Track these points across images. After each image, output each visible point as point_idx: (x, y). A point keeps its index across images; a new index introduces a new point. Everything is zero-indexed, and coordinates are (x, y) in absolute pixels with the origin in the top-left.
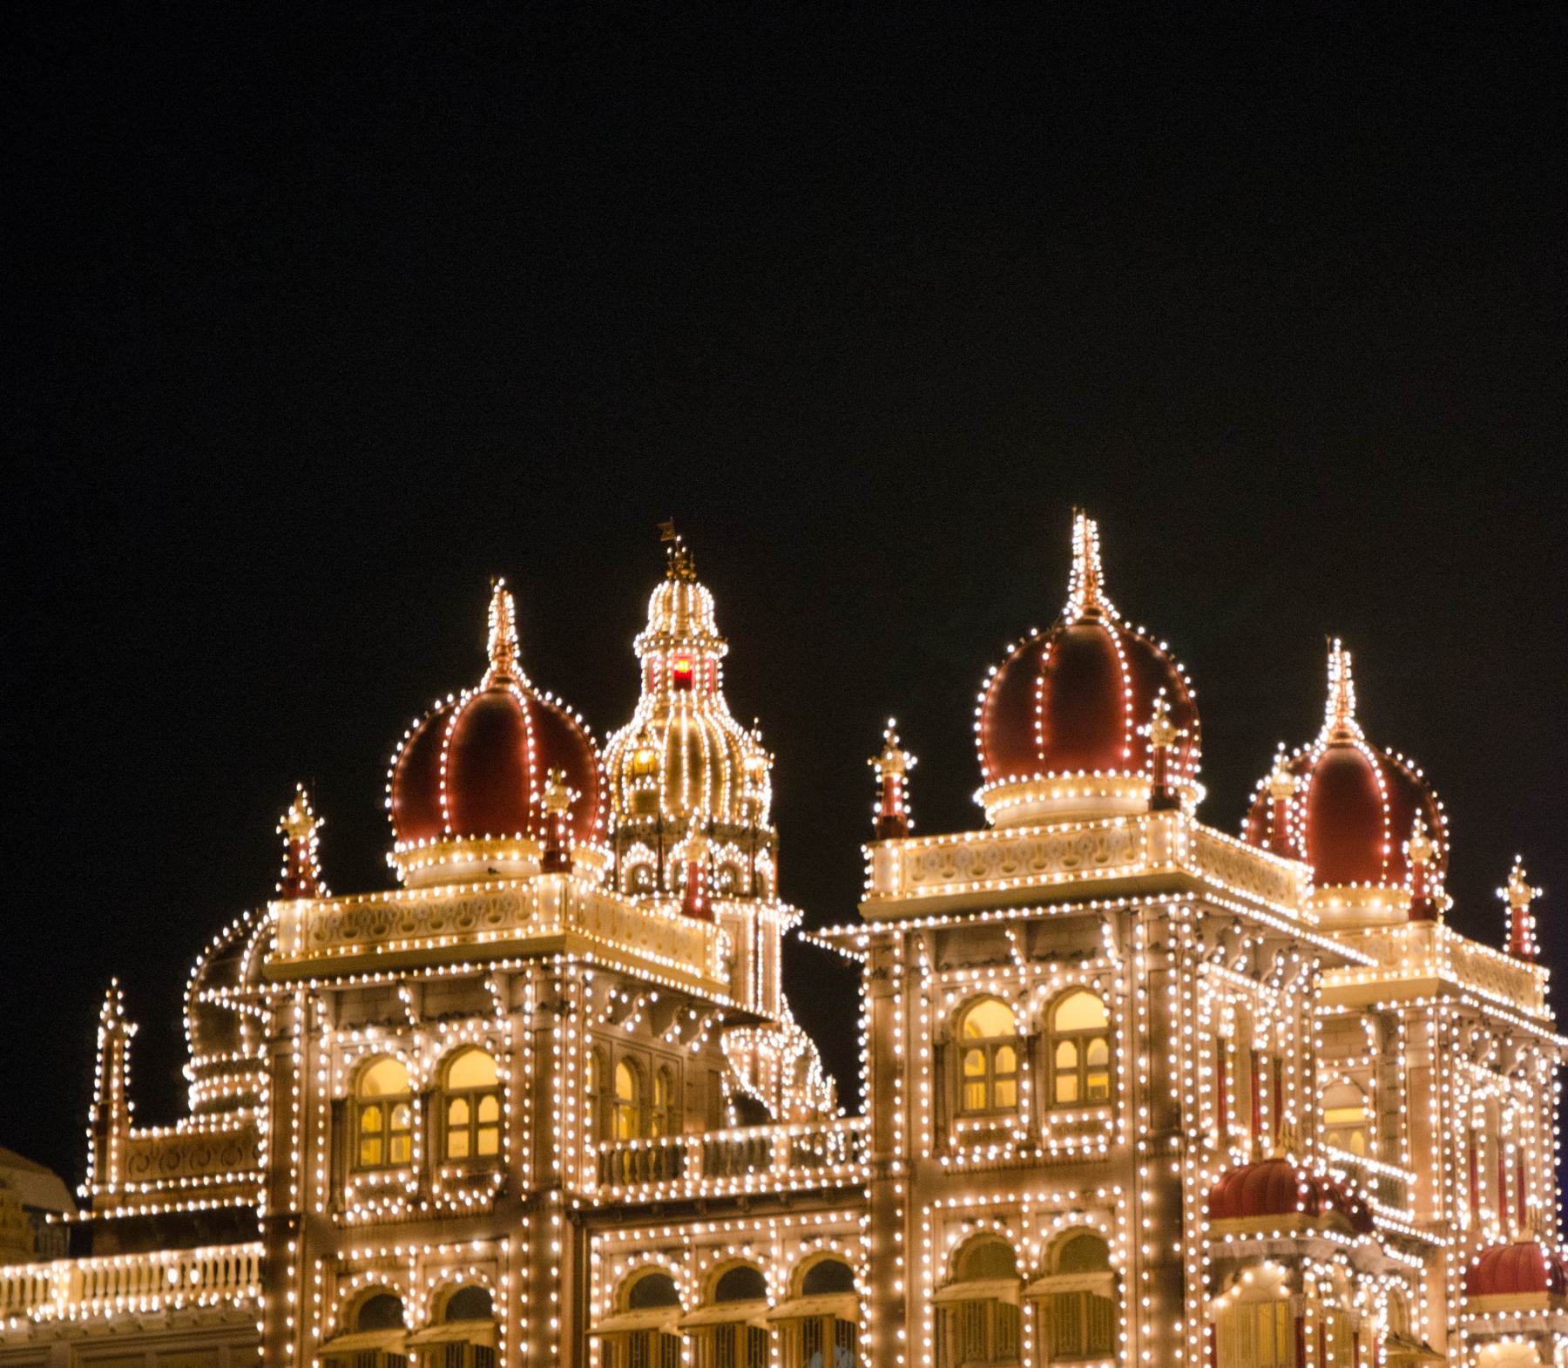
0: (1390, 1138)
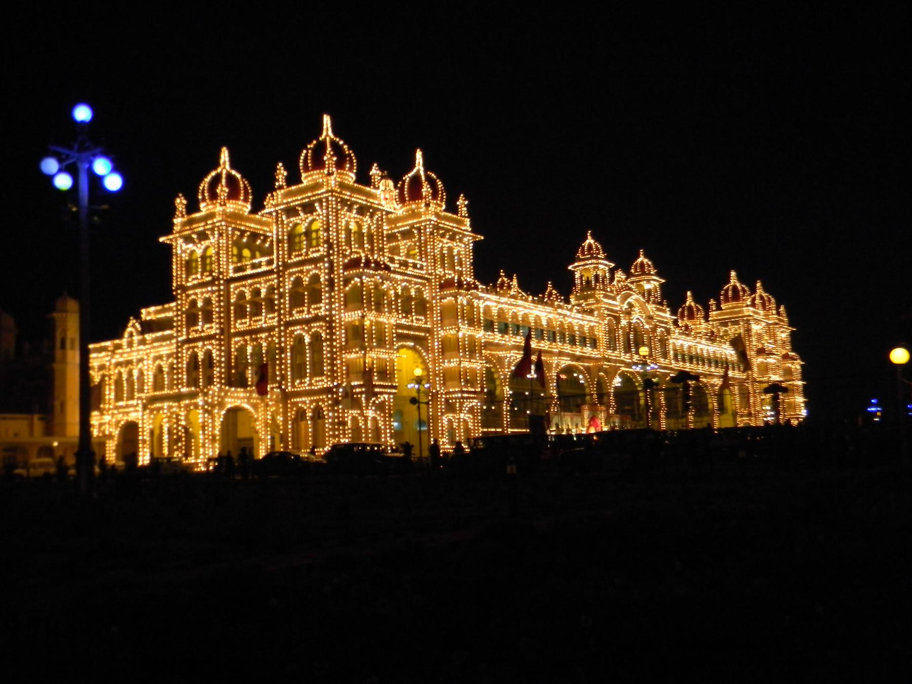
0: (421, 255)
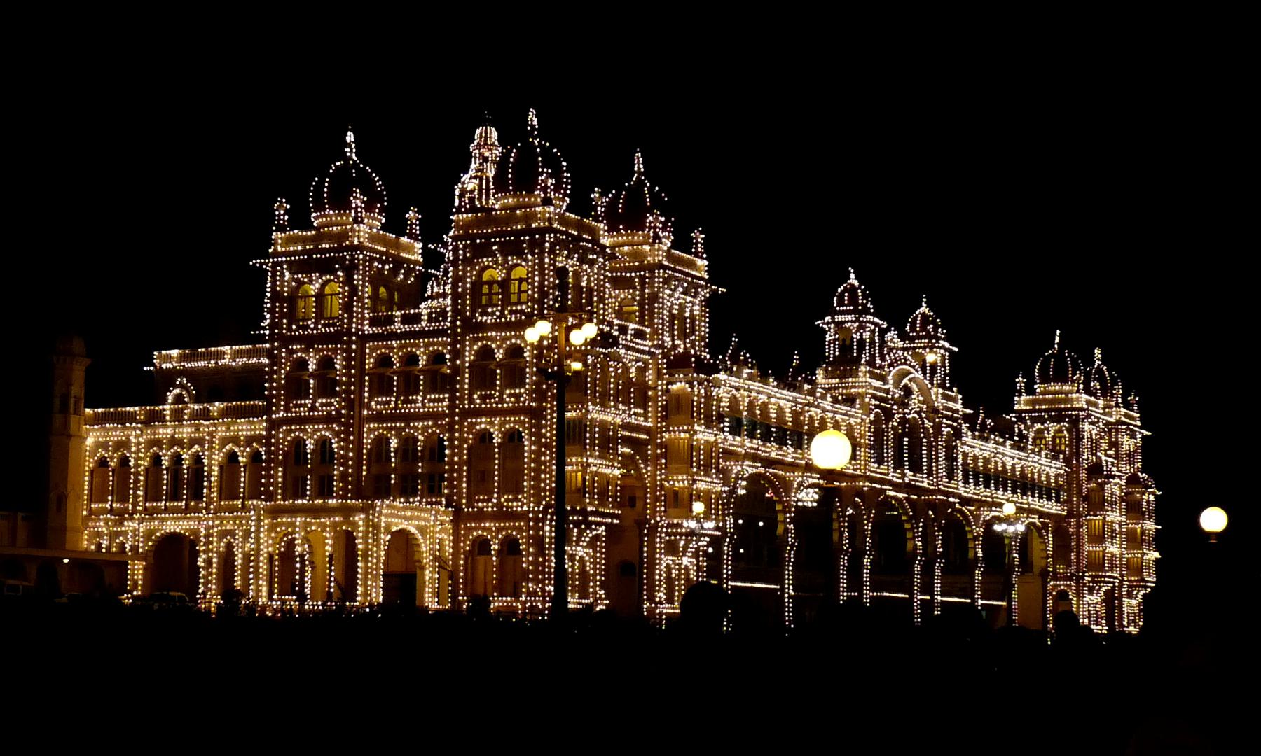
0: (642, 317)
